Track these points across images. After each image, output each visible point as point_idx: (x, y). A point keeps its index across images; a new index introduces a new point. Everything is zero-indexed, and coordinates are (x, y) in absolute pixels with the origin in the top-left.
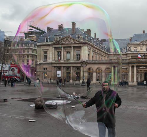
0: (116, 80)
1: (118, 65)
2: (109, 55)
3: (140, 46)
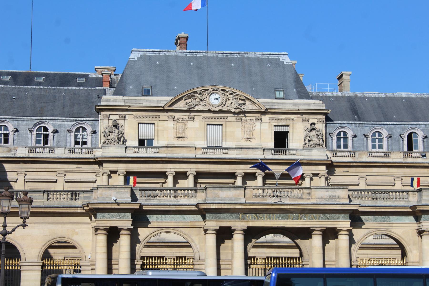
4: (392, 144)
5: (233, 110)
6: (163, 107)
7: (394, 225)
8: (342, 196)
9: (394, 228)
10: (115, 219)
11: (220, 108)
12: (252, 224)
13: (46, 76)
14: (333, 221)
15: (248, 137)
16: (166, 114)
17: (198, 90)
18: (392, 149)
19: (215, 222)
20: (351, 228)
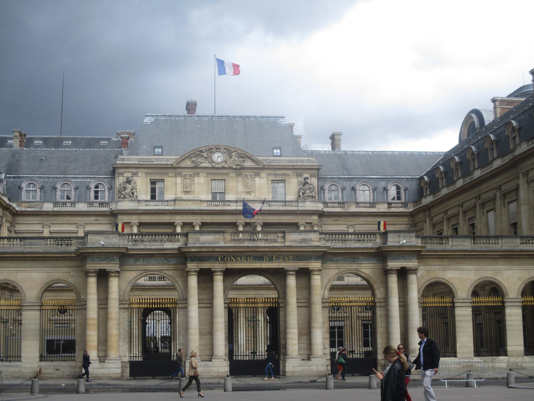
0: (113, 354)
1: (121, 265)
2: (15, 214)
3: (180, 174)
4: (377, 195)
5: (234, 167)
6: (172, 165)
7: (362, 265)
10: (104, 262)
11: (223, 164)
13: (73, 140)
15: (248, 190)
16: (175, 171)
17: (203, 149)
18: (377, 200)
19: (196, 265)
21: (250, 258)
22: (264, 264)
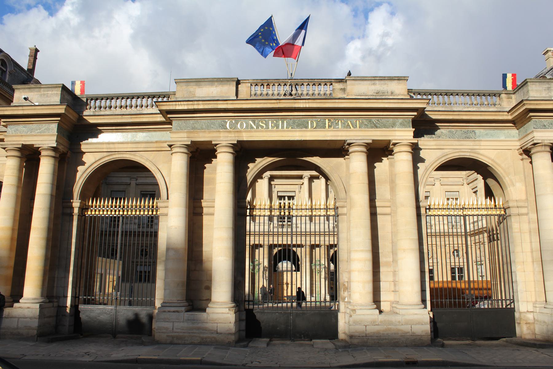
7: (482, 143)
8: (397, 92)
9: (482, 147)
12: (246, 137)
14: (384, 129)
19: (185, 135)
20: (415, 141)
21: (283, 123)
22: (308, 134)
